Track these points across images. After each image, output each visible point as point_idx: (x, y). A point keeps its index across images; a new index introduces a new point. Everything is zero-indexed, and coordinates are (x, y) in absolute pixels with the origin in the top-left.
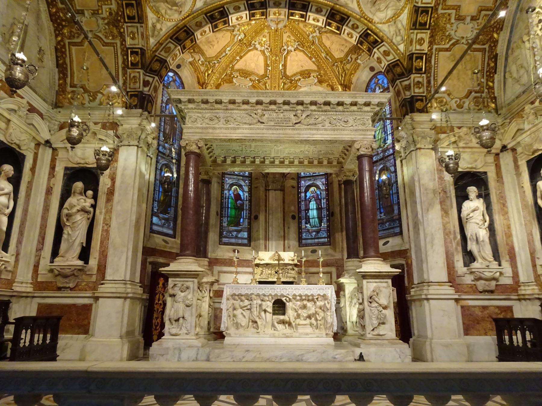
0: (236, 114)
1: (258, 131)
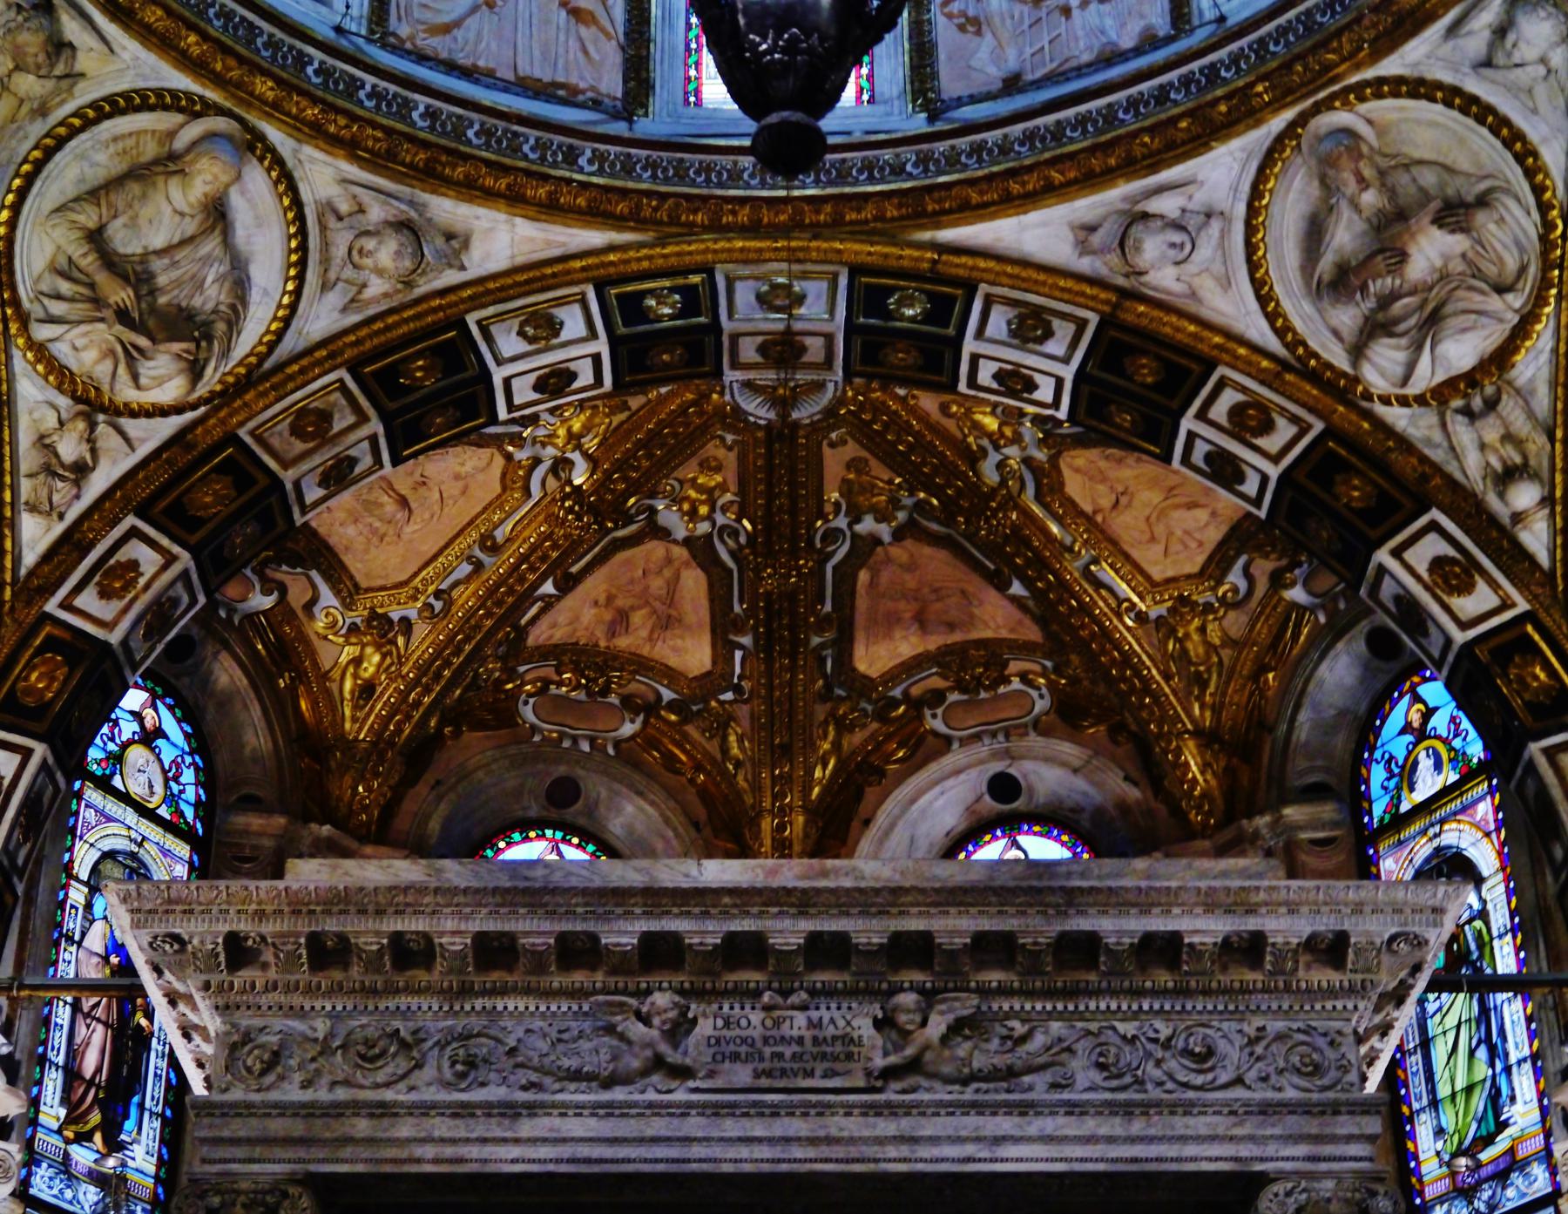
0: (521, 1015)
1: (658, 1126)
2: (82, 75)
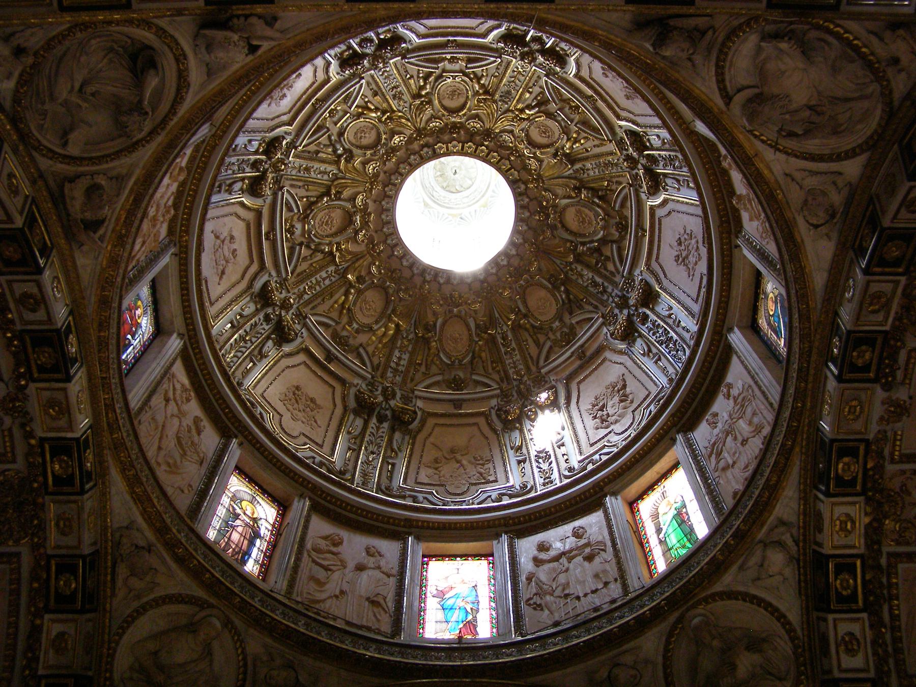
2: (159, 584)
